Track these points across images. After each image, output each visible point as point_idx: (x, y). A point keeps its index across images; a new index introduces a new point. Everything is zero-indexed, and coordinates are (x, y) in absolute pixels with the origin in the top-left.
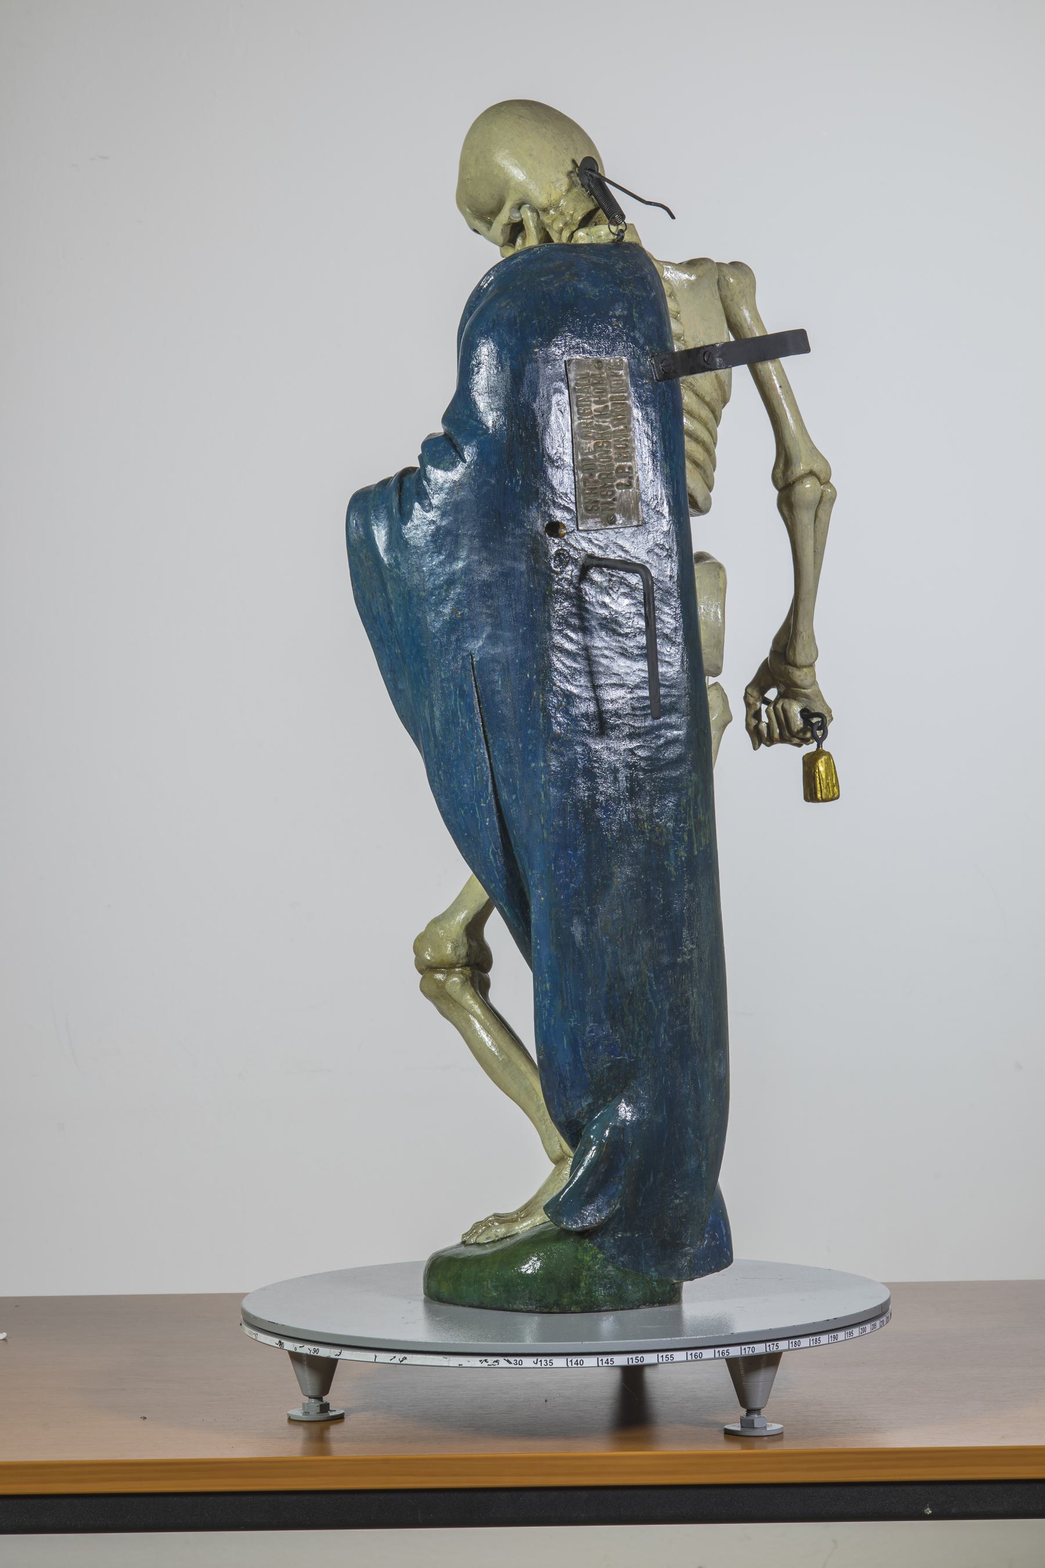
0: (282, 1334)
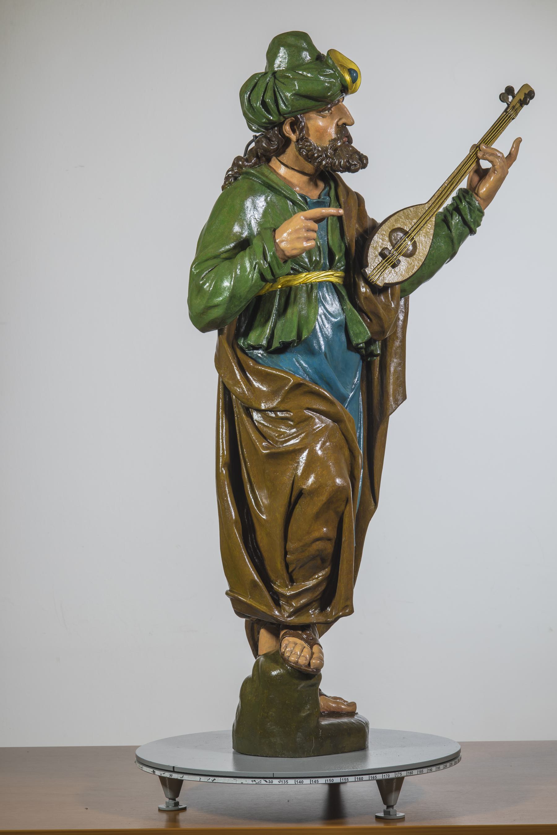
0: (155, 767)
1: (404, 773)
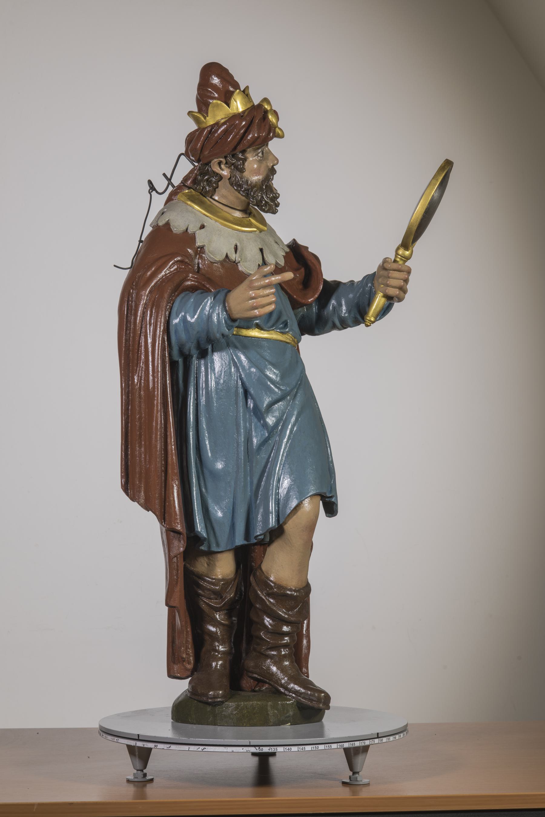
1: (376, 741)
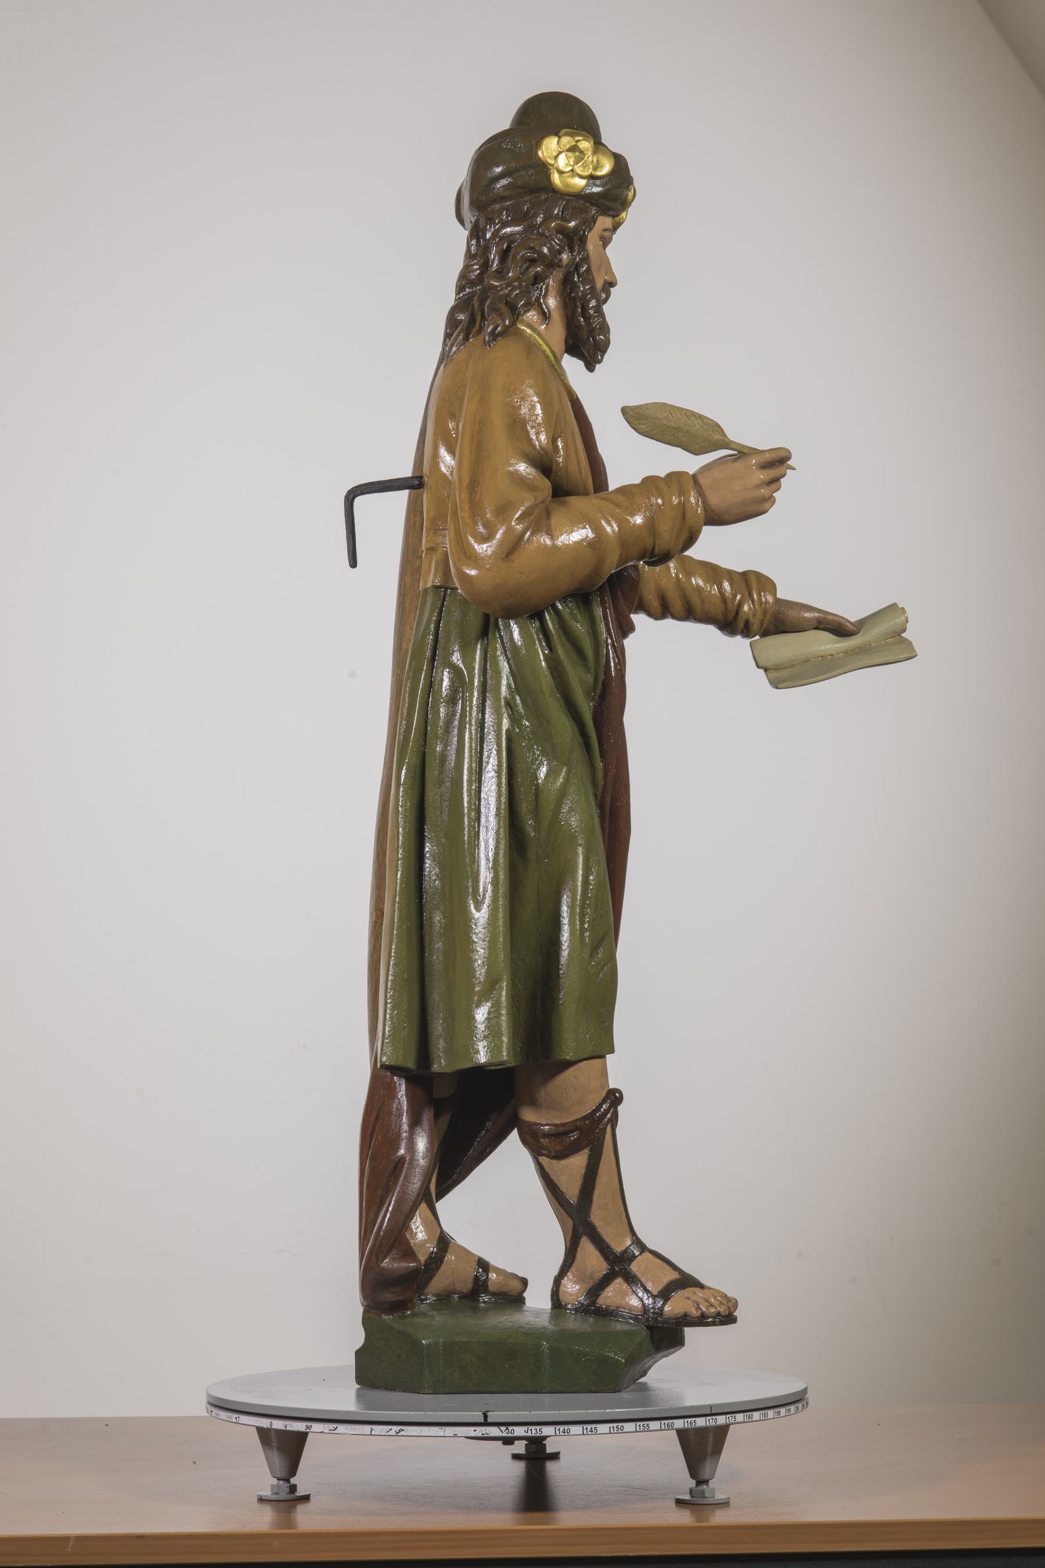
1: (740, 1417)
